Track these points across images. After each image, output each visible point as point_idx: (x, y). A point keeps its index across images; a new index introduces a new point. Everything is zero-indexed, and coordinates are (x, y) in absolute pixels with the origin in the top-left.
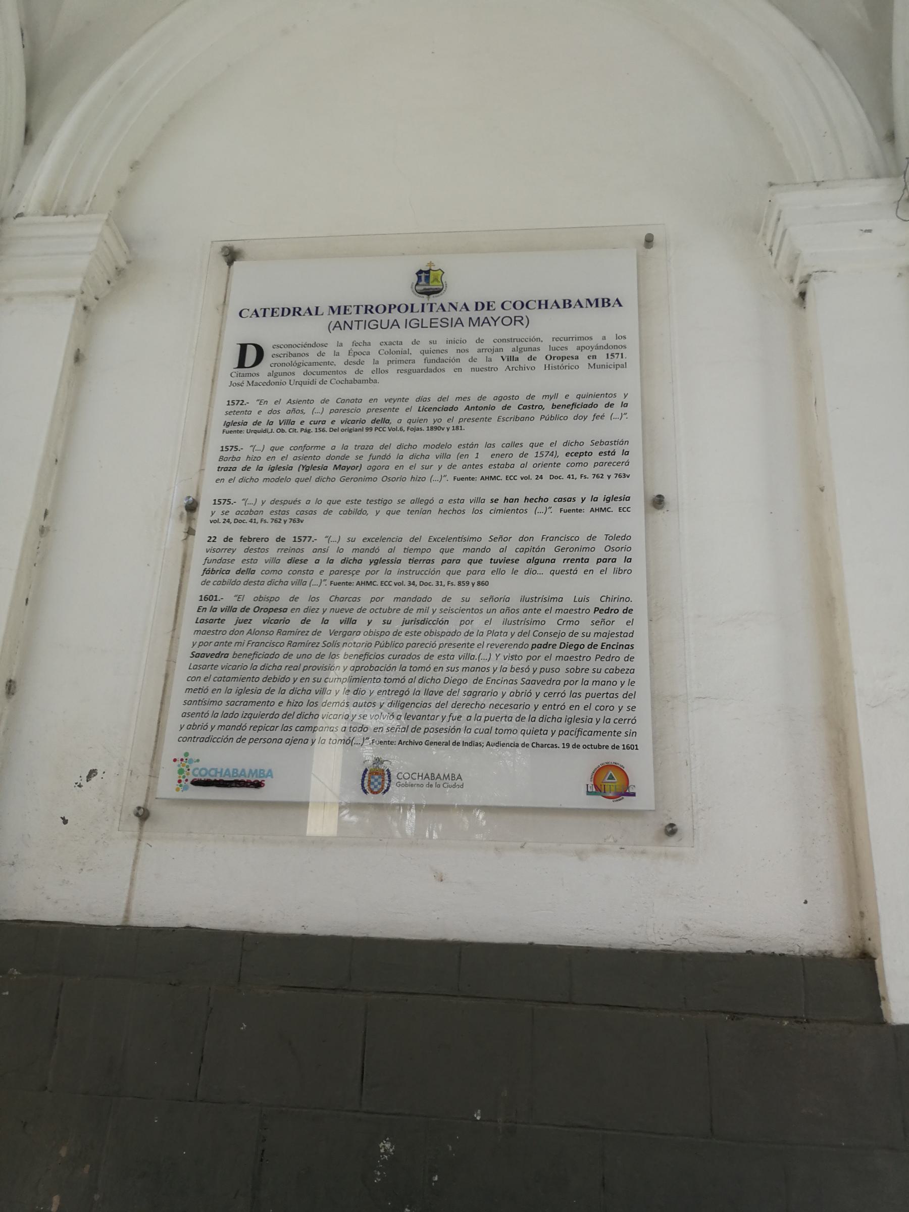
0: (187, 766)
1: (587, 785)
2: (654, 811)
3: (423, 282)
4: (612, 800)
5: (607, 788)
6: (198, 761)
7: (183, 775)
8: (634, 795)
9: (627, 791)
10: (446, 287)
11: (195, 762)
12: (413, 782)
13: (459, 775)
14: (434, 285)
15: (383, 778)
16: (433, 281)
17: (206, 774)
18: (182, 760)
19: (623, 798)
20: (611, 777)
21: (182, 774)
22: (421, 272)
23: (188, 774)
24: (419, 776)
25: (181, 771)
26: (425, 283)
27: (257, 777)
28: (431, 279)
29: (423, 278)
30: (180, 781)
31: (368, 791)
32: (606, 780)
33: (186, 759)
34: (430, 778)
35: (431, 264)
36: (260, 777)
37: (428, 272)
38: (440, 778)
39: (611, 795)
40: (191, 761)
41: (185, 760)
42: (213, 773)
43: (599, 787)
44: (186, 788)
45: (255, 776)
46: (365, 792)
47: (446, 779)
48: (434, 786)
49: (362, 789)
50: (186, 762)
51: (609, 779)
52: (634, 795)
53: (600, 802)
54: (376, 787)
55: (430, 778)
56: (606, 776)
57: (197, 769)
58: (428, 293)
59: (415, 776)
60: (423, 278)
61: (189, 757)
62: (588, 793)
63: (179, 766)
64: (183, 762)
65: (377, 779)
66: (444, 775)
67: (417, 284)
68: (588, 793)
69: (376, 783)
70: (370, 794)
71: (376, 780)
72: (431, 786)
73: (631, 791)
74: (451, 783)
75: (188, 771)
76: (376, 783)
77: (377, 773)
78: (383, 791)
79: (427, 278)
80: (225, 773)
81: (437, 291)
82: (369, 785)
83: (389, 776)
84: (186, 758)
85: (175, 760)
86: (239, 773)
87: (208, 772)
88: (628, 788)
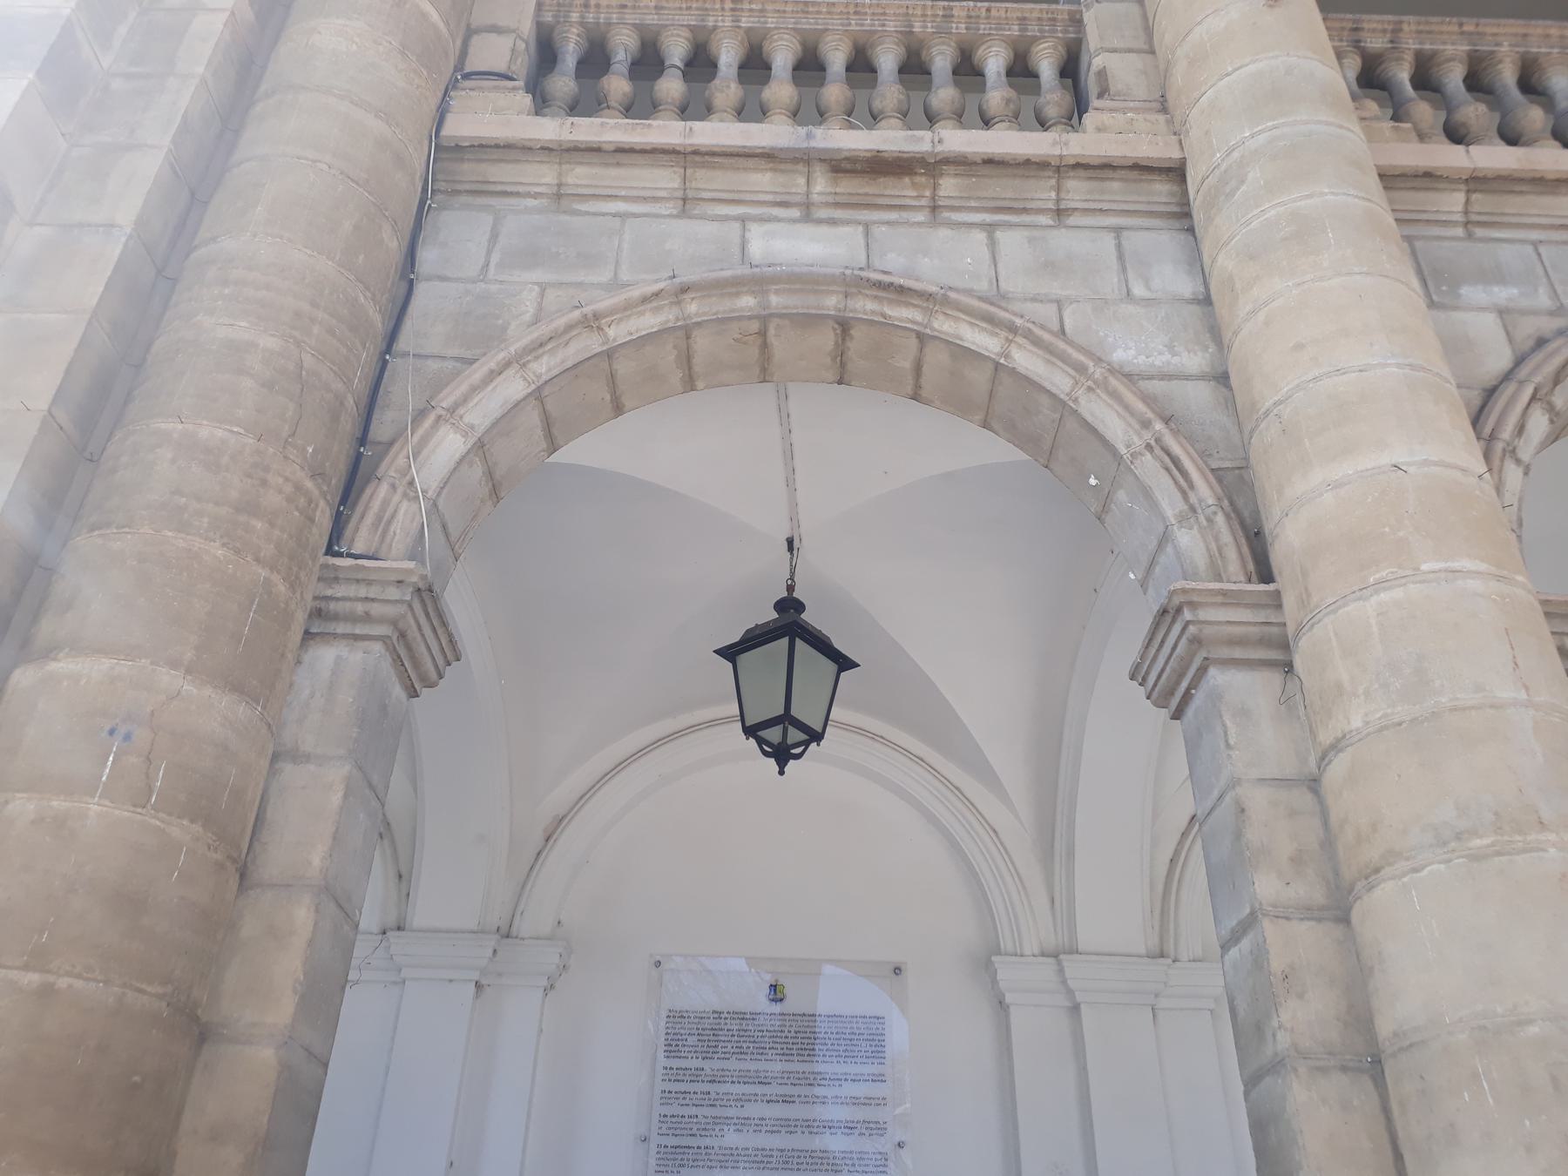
14: (779, 996)
28: (778, 991)
37: (775, 986)
79: (775, 990)
81: (781, 1000)
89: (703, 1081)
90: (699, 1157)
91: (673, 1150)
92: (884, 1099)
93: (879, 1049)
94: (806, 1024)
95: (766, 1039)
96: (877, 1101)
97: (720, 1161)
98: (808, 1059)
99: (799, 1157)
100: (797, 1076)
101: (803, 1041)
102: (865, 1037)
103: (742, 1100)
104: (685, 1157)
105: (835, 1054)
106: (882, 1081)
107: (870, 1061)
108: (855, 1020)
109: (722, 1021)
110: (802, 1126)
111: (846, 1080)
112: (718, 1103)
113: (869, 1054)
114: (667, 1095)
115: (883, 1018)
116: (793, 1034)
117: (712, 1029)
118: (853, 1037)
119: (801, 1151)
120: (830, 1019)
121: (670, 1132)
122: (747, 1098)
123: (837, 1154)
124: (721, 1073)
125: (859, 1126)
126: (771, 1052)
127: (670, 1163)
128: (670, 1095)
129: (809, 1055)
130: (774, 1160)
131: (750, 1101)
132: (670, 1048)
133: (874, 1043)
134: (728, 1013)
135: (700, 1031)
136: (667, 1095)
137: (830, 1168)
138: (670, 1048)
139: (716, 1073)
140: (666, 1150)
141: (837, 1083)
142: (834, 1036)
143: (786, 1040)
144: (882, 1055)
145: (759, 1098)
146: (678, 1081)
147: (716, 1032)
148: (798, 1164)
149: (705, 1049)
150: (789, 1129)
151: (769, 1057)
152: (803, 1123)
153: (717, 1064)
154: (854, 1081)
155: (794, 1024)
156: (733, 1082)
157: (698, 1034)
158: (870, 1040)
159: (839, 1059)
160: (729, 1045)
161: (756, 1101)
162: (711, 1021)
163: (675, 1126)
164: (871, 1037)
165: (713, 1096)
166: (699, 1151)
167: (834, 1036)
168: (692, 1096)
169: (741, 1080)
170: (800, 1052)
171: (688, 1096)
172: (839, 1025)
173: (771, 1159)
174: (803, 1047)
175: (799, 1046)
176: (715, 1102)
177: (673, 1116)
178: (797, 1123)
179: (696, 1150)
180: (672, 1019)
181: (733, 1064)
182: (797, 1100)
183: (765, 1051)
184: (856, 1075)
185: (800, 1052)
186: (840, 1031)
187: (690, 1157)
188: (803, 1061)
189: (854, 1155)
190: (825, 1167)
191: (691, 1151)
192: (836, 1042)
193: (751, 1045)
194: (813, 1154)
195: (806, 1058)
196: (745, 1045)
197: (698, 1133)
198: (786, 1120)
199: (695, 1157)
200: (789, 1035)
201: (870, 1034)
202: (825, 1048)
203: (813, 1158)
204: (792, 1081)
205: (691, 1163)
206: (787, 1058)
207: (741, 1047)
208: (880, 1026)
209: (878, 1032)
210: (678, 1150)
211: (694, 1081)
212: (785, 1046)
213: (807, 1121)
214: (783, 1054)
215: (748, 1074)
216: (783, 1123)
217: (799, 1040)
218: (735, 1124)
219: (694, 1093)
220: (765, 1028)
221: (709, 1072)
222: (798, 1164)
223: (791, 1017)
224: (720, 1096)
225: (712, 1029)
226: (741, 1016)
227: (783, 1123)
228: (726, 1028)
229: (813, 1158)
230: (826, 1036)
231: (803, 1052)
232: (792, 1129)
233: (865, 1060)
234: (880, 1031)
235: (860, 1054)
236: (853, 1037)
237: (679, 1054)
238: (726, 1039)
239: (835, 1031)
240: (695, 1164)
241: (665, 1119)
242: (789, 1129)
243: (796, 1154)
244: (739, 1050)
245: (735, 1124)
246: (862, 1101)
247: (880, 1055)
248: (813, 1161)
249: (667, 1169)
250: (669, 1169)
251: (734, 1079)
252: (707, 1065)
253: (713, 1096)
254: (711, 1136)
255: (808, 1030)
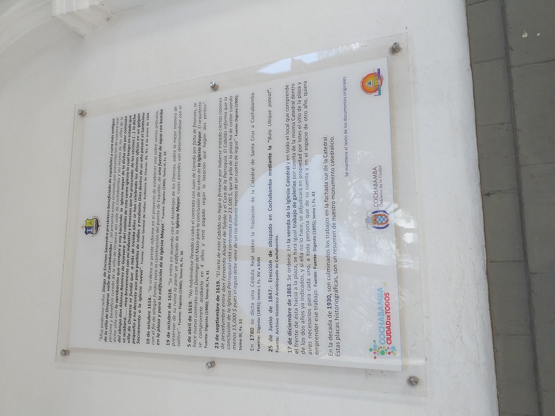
0: (379, 348)
1: (375, 96)
2: (387, 57)
3: (91, 230)
4: (383, 81)
5: (376, 84)
6: (374, 341)
7: (385, 351)
8: (379, 70)
9: (377, 73)
10: (95, 216)
11: (375, 343)
12: (379, 196)
13: (373, 169)
14: (94, 224)
15: (378, 215)
16: (91, 224)
17: (384, 335)
18: (375, 353)
19: (381, 75)
20: (370, 83)
21: (385, 352)
22: (86, 233)
23: (384, 347)
24: (375, 194)
25: (383, 353)
26: (92, 229)
27: (383, 299)
28: (90, 225)
29: (89, 230)
30: (389, 353)
31: (387, 224)
32: (371, 86)
33: (374, 350)
34: (376, 186)
35: (82, 227)
36: (383, 297)
37: (86, 228)
38: (376, 180)
39: (380, 82)
40: (375, 346)
41: (375, 351)
42: (382, 330)
43: (375, 89)
44: (394, 348)
45: (382, 300)
46: (387, 226)
47: (376, 176)
48: (381, 183)
49: (386, 228)
50: (376, 350)
51: (371, 85)
52: (379, 70)
53: (385, 88)
54: (384, 219)
55: (376, 186)
56: (369, 86)
57: (380, 341)
58: (97, 226)
59: (376, 196)
60: (89, 230)
61: (373, 348)
62: (380, 94)
63: (379, 355)
64: (376, 352)
65: (379, 220)
66: (374, 178)
67: (92, 233)
68: (380, 94)
69: (382, 219)
70: (389, 223)
71: (380, 220)
72: (381, 185)
73: (376, 71)
74: (378, 173)
75: (382, 348)
76: (382, 219)
77: (375, 220)
78: (386, 214)
79: (90, 228)
80: (381, 321)
82: (383, 224)
83: (377, 212)
84: (373, 350)
85: (375, 358)
86: (381, 311)
87: (382, 333)
88: (375, 73)
89: (160, 298)
90: (226, 298)
91: (220, 328)
92: (176, 109)
93: (137, 119)
94: (116, 193)
95: (127, 233)
96: (178, 116)
97: (230, 273)
98: (143, 188)
99: (225, 188)
100: (157, 198)
101: (129, 195)
102: (127, 135)
103: (177, 255)
104: (226, 314)
105: (139, 162)
106: (161, 113)
107: (145, 127)
108: (114, 147)
109: (111, 280)
110: (199, 188)
111: (160, 149)
112: (179, 281)
113: (141, 128)
114: (171, 339)
115: (114, 120)
116: (123, 206)
117: (117, 291)
118: (127, 147)
119: (220, 185)
120: (113, 171)
121: (204, 333)
122: (175, 248)
123: (222, 149)
124: (153, 280)
125: (198, 130)
126: (137, 228)
127: (232, 332)
128: (171, 335)
129: (140, 189)
130: (228, 214)
131: (177, 247)
132: (131, 337)
133: (132, 126)
134: (105, 275)
135: (119, 304)
136: (171, 339)
137: (234, 155)
138: (131, 337)
139: (153, 285)
140: (220, 338)
141: (163, 157)
142: (126, 165)
143: (128, 212)
144: (141, 116)
145: (175, 236)
146: (159, 326)
147: (120, 287)
148: (231, 189)
149: (133, 298)
150: (201, 201)
151: (141, 228)
152: (196, 188)
153: (146, 285)
154: (161, 140)
155: (115, 206)
156: (161, 265)
157: (121, 306)
158: (130, 130)
159: (144, 158)
160: (130, 271)
161: (177, 239)
162: (110, 292)
163: (198, 328)
164: (128, 129)
165: (172, 286)
166: (221, 298)
167: (126, 165)
168: (172, 310)
169: (159, 256)
170: (138, 198)
171: (172, 314)
172: (117, 162)
173: (228, 217)
174: (133, 195)
175: (133, 198)
176: (178, 283)
177: (190, 330)
178: (196, 193)
179: (220, 302)
180: (108, 336)
181: (146, 267)
182: (177, 195)
183: (136, 233)
184: (156, 138)
185: (138, 198)
186: (122, 159)
187: (226, 308)
188: (145, 193)
189: (223, 132)
190: (233, 160)
191: (221, 307)
192: (131, 162)
193: (131, 248)
194: (223, 174)
195: (143, 191)
196: (131, 255)
197: (205, 301)
198: (194, 206)
199: (226, 303)
200: (124, 209)
201: (125, 130)
202: (135, 172)
203: (226, 174)
204: (161, 203)
205: (232, 307)
206: (142, 209)
207: (133, 259)
208: (120, 121)
209: (124, 123)
210: (220, 324)
211: (160, 308)
212: (133, 213)
213: (194, 183)
214: (139, 214)
215: (154, 250)
216: (196, 208)
217: (129, 199)
218: (197, 260)
219: (169, 307)
220: (118, 235)
221: (152, 293)
222: (231, 189)
223: (111, 209)
224: (173, 278)
225: (117, 291)
226: (108, 260)
227: (196, 208)
228: (116, 276)
229: (226, 174)
230: (126, 173)
231: (138, 194)
232: (201, 198)
233: (145, 133)
234: (123, 121)
235: (140, 138)
236: (127, 147)
237: (137, 326)
238: (125, 275)
239: (122, 164)
240: (232, 301)
241: (192, 339)
242: (201, 201)
243: (223, 191)
244: (135, 260)
245: (197, 260)
246: (177, 130)
247: (141, 118)
248: (228, 173)
249: (237, 335)
250: (238, 332)
251: (159, 264)
252: (146, 295)
253: (172, 286)
254: (207, 286)
255: (121, 191)
